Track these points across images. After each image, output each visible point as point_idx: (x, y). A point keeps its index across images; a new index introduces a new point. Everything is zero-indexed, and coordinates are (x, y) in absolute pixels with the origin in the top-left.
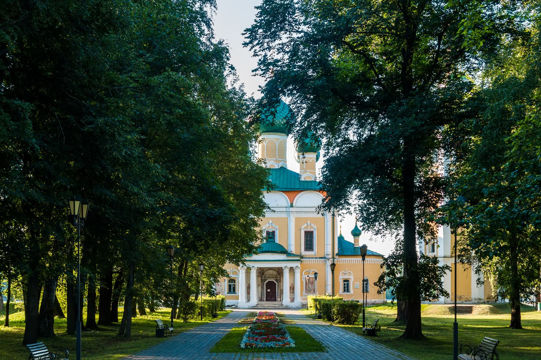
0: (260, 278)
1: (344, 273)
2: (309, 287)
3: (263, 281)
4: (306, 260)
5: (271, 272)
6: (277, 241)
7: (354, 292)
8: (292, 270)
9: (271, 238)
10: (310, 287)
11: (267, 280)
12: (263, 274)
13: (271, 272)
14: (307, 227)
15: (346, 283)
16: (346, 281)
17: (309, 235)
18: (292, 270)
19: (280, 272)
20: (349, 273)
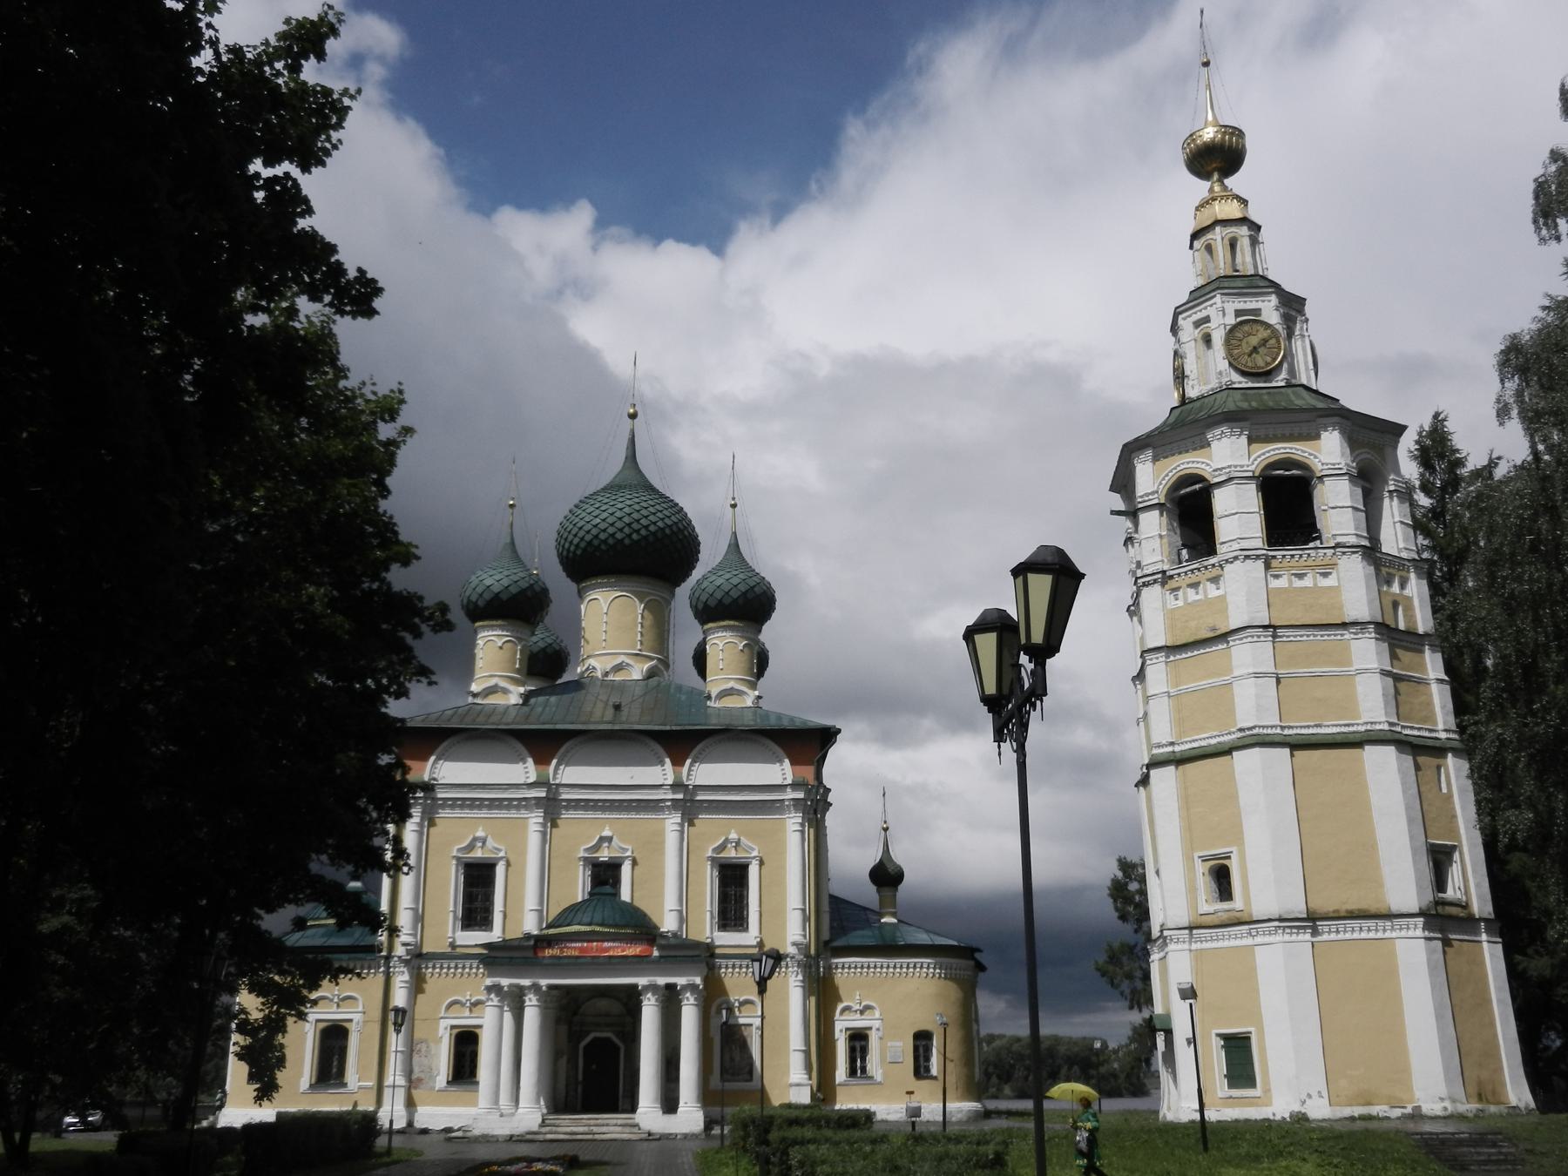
0: (564, 1029)
1: (847, 1009)
2: (732, 1060)
3: (574, 1037)
4: (723, 962)
5: (603, 1004)
6: (625, 895)
7: (885, 1074)
8: (670, 1000)
9: (604, 883)
10: (737, 1058)
11: (588, 1033)
12: (575, 1013)
13: (603, 1004)
14: (722, 847)
15: (858, 1045)
16: (858, 1039)
17: (732, 877)
18: (670, 1000)
19: (630, 999)
20: (868, 1008)
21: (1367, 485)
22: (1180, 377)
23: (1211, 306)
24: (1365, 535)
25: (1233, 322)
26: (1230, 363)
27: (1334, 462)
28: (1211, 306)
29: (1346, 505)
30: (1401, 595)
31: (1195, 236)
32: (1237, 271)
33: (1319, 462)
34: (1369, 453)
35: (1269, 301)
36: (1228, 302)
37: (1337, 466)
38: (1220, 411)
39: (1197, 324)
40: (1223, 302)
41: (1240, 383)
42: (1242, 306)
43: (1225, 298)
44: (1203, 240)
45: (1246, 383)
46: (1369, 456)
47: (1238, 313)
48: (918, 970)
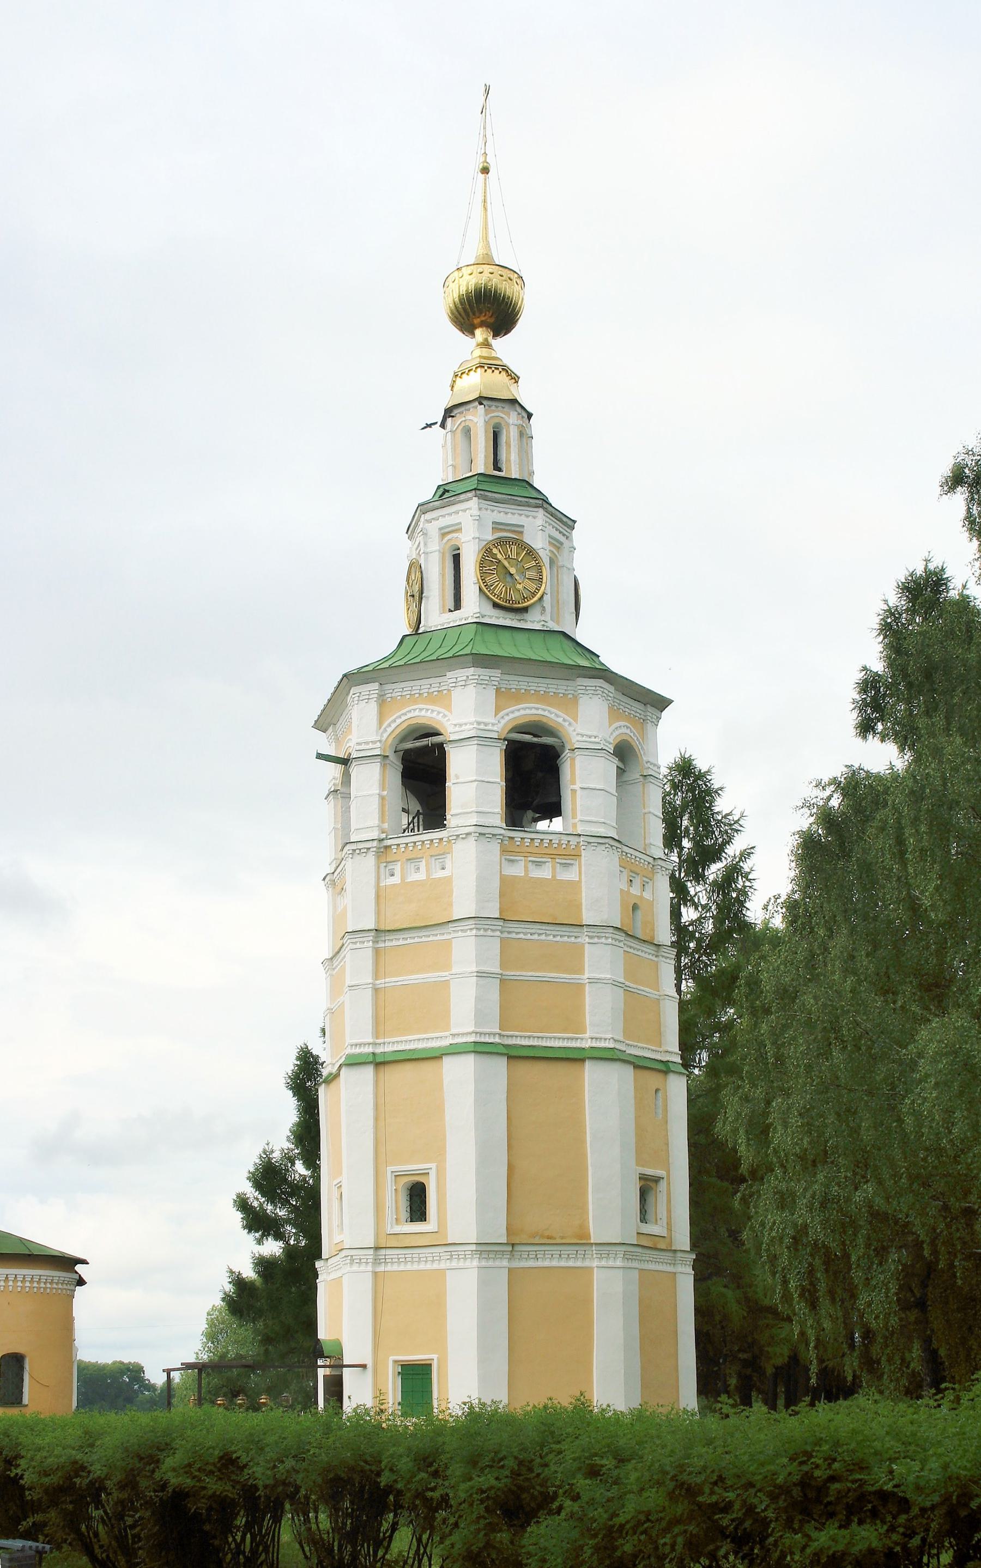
21: (621, 766)
22: (417, 596)
23: (465, 511)
24: (615, 825)
25: (490, 537)
26: (480, 589)
27: (589, 733)
28: (465, 511)
29: (598, 787)
30: (641, 897)
31: (449, 413)
32: (500, 470)
33: (574, 730)
34: (628, 728)
35: (534, 517)
36: (487, 509)
37: (593, 739)
38: (467, 651)
39: (444, 532)
40: (480, 509)
41: (491, 617)
42: (501, 518)
44: (459, 420)
45: (498, 618)
47: (497, 526)
48: (11, 1283)
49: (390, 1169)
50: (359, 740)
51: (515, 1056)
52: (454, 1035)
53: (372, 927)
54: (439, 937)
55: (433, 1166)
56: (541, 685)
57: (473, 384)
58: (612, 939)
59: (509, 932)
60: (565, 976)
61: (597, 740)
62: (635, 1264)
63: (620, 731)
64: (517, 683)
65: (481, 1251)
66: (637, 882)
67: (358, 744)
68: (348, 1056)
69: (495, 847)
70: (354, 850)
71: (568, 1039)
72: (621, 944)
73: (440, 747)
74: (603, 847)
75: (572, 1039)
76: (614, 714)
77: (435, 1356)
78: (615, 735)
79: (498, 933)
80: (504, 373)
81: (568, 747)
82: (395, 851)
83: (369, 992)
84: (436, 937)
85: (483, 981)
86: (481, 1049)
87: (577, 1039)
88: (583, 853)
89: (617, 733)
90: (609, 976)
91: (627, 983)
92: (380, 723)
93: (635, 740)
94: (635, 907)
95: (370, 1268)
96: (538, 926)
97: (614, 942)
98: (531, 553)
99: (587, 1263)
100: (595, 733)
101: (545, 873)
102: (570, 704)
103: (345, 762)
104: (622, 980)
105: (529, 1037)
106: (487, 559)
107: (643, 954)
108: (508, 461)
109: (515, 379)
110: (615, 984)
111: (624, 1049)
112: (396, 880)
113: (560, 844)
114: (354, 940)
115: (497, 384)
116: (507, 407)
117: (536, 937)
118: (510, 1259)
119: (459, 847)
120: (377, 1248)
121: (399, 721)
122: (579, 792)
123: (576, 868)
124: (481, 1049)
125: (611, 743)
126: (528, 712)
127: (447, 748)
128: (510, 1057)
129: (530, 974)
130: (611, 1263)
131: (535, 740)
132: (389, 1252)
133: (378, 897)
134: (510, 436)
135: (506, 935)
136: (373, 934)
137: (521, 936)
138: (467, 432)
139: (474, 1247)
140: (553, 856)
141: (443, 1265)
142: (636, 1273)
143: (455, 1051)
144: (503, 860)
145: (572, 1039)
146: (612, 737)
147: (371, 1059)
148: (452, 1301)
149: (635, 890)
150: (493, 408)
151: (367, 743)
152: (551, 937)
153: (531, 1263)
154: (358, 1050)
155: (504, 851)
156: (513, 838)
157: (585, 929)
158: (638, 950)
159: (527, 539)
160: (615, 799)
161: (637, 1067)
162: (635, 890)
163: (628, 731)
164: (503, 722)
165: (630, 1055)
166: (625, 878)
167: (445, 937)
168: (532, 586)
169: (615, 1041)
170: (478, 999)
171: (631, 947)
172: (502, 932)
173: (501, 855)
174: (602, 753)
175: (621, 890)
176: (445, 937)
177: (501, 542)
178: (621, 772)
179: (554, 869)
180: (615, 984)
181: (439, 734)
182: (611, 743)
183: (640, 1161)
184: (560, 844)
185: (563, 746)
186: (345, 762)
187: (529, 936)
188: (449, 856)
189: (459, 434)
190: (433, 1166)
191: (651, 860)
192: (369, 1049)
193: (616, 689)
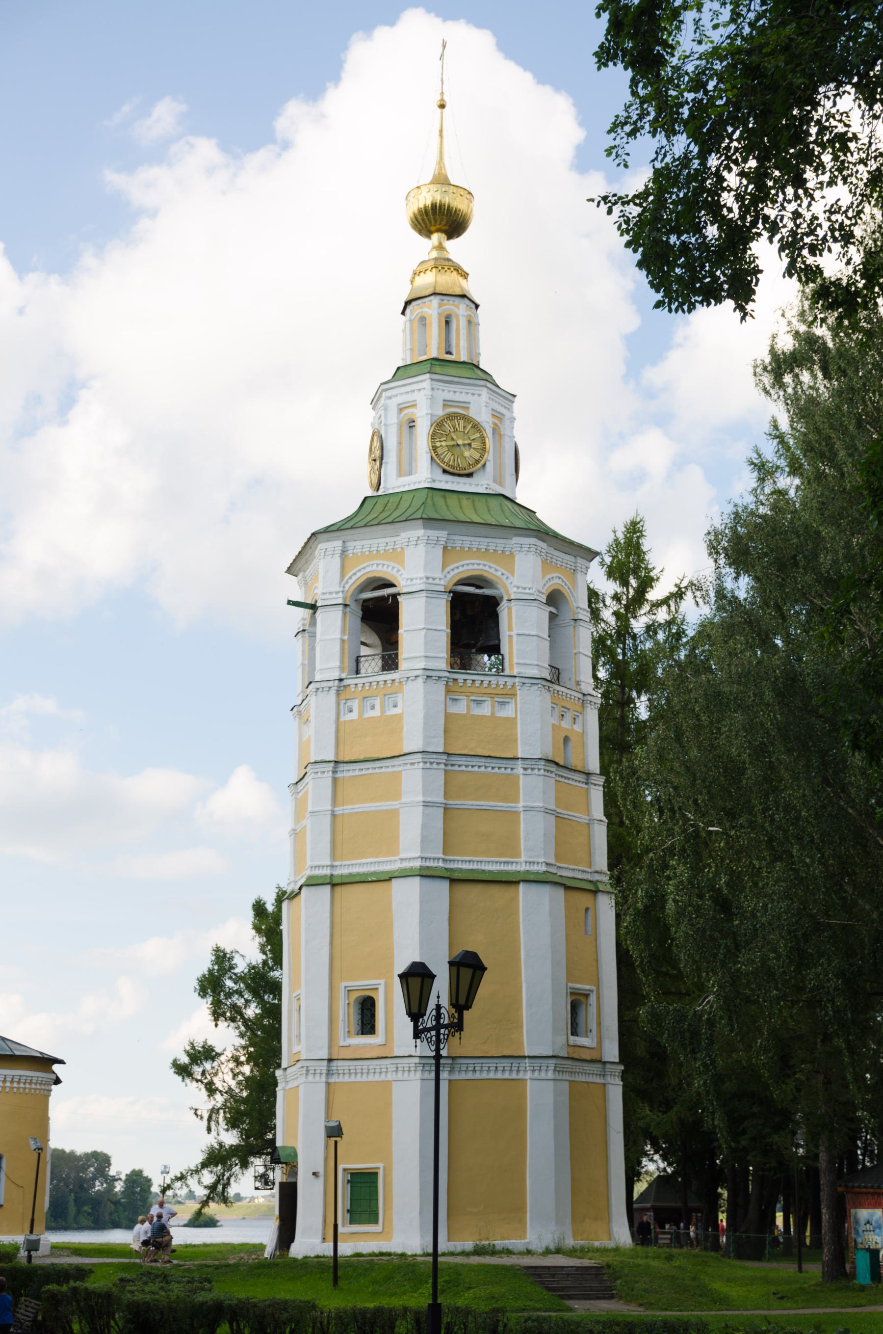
26: (432, 458)
27: (524, 586)
30: (573, 730)
37: (527, 591)
43: (437, 385)
46: (560, 582)
49: (344, 984)
50: (325, 591)
51: (455, 880)
52: (402, 860)
53: (332, 758)
54: (390, 769)
55: (382, 982)
56: (483, 543)
57: (428, 279)
58: (545, 770)
59: (452, 765)
60: (501, 804)
61: (531, 591)
62: (566, 1077)
63: (552, 582)
64: (462, 541)
65: (424, 1064)
66: (569, 716)
67: (324, 594)
68: (310, 878)
69: (441, 687)
70: (318, 689)
71: (505, 863)
72: (553, 775)
73: (395, 596)
74: (536, 687)
75: (508, 863)
76: (547, 565)
77: (381, 1165)
78: (548, 585)
79: (442, 766)
80: (455, 273)
81: (505, 598)
82: (353, 690)
83: (328, 819)
84: (389, 767)
85: (429, 810)
86: (426, 874)
87: (512, 863)
88: (518, 692)
89: (550, 583)
90: (541, 805)
91: (559, 810)
92: (343, 575)
93: (566, 591)
94: (566, 740)
95: (324, 1078)
96: (478, 759)
97: (546, 773)
98: (476, 427)
99: (521, 1075)
100: (529, 585)
101: (485, 710)
102: (507, 559)
103: (313, 607)
104: (553, 807)
105: (470, 861)
106: (438, 429)
107: (574, 783)
108: (458, 345)
109: (465, 275)
110: (547, 811)
111: (555, 871)
112: (354, 716)
113: (497, 685)
114: (316, 770)
115: (448, 281)
116: (457, 300)
117: (476, 769)
118: (450, 1071)
119: (408, 687)
120: (330, 1060)
121: (359, 575)
122: (515, 638)
123: (511, 706)
124: (426, 874)
125: (543, 593)
126: (470, 567)
127: (400, 598)
128: (453, 881)
129: (471, 803)
130: (543, 1075)
131: (478, 591)
132: (340, 1063)
133: (337, 731)
134: (460, 325)
135: (449, 768)
136: (332, 764)
137: (463, 768)
138: (423, 320)
139: (417, 1060)
140: (492, 695)
141: (390, 1077)
142: (567, 1084)
143: (405, 874)
144: (448, 700)
145: (508, 863)
146: (546, 588)
147: (328, 881)
148: (397, 1112)
149: (565, 724)
150: (445, 302)
151: (331, 593)
152: (490, 769)
153: (470, 1076)
154: (317, 872)
155: (448, 691)
156: (456, 680)
157: (520, 761)
158: (569, 779)
159: (472, 413)
160: (547, 644)
161: (567, 888)
162: (565, 724)
163: (560, 582)
164: (449, 576)
165: (561, 876)
166: (557, 713)
167: (395, 769)
168: (477, 456)
169: (547, 864)
170: (424, 827)
171: (562, 776)
172: (446, 765)
173: (446, 695)
174: (535, 603)
175: (553, 725)
176: (395, 769)
177: (451, 417)
178: (553, 617)
179: (493, 706)
180: (547, 811)
181: (392, 585)
182: (543, 593)
183: (570, 976)
184: (497, 685)
185: (502, 598)
186: (313, 607)
187: (470, 769)
188: (400, 695)
189: (416, 324)
190: (382, 982)
191: (580, 696)
192: (327, 872)
193: (548, 545)
